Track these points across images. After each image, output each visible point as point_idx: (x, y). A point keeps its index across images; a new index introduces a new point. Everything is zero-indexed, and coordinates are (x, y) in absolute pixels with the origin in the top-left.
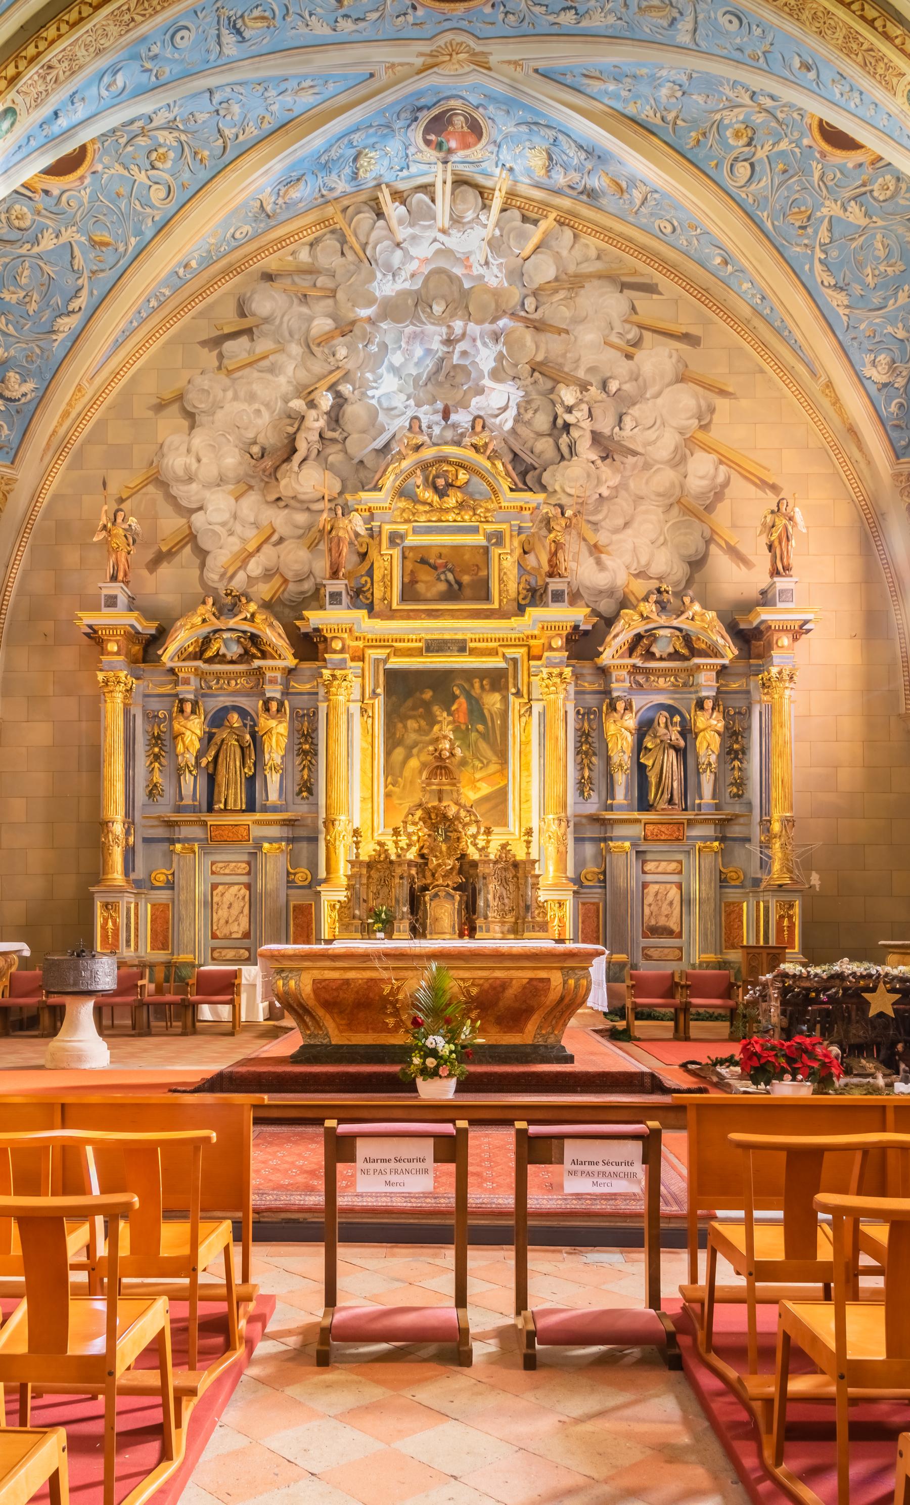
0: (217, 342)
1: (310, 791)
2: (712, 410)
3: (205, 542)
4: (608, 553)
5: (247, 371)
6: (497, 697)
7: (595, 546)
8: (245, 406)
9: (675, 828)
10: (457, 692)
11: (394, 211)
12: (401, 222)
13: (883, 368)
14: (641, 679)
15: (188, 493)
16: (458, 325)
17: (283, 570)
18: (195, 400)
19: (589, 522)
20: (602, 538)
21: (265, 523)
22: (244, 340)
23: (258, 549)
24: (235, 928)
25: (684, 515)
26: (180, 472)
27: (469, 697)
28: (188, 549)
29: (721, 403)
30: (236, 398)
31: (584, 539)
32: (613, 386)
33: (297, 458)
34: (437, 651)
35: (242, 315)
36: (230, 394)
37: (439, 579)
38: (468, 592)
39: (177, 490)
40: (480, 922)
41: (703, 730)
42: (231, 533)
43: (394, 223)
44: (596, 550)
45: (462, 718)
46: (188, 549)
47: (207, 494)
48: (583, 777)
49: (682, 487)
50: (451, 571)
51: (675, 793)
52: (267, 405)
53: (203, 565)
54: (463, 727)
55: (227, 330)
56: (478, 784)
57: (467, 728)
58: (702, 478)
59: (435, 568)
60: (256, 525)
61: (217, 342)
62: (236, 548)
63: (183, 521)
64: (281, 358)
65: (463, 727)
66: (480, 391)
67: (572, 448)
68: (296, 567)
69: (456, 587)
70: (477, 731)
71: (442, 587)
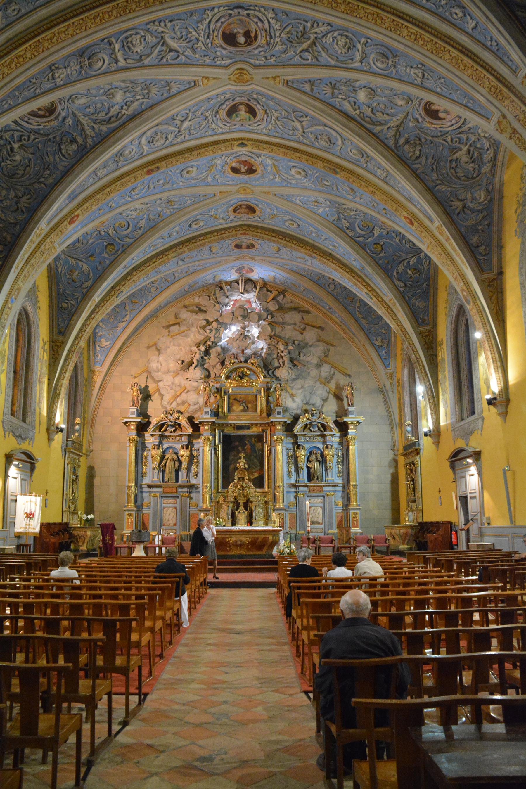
0: (168, 327)
1: (197, 475)
2: (329, 351)
3: (163, 392)
5: (178, 336)
8: (177, 348)
11: (226, 288)
12: (228, 290)
13: (380, 341)
14: (307, 438)
15: (158, 375)
16: (246, 323)
17: (189, 401)
18: (161, 345)
20: (294, 391)
21: (183, 386)
22: (177, 327)
23: (180, 394)
24: (171, 522)
26: (155, 368)
27: (251, 444)
28: (157, 394)
29: (332, 349)
30: (174, 345)
32: (296, 343)
33: (194, 365)
35: (176, 318)
36: (172, 344)
38: (250, 410)
39: (154, 374)
40: (254, 520)
42: (172, 389)
43: (226, 291)
44: (292, 395)
45: (248, 451)
46: (157, 394)
47: (164, 376)
49: (320, 375)
52: (184, 347)
53: (162, 399)
55: (171, 323)
59: (239, 401)
60: (180, 386)
61: (168, 327)
62: (173, 394)
63: (155, 385)
64: (190, 332)
66: (254, 343)
67: (283, 363)
68: (193, 400)
71: (242, 408)
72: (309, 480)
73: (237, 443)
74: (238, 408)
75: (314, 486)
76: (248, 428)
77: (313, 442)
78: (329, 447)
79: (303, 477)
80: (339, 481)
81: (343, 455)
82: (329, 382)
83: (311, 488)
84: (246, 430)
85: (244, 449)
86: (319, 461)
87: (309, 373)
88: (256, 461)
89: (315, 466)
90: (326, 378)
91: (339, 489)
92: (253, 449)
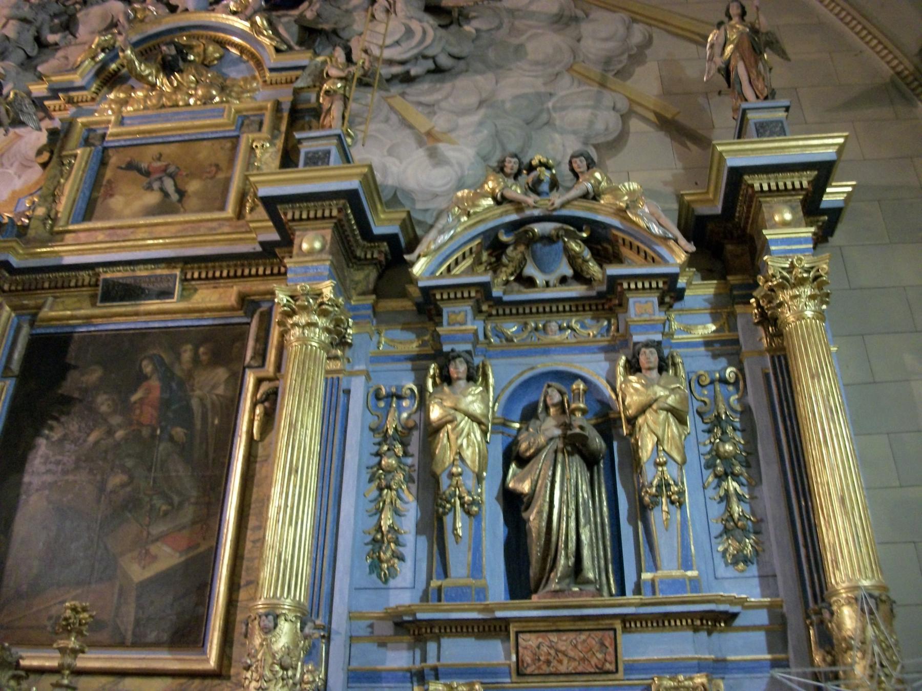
4: (451, 142)
6: (221, 373)
7: (429, 134)
9: (593, 640)
10: (148, 368)
19: (420, 104)
20: (440, 123)
25: (580, 83)
27: (167, 375)
31: (410, 127)
34: (122, 299)
37: (149, 188)
41: (642, 411)
48: (379, 529)
50: (172, 176)
51: (586, 552)
54: (145, 432)
56: (153, 549)
57: (153, 436)
58: (606, 40)
59: (147, 174)
65: (145, 432)
69: (175, 197)
70: (171, 439)
71: (153, 198)
72: (521, 584)
73: (94, 375)
74: (129, 202)
75: (552, 626)
76: (166, 294)
77: (546, 350)
78: (649, 358)
79: (476, 568)
80: (742, 588)
81: (746, 412)
82: (623, 74)
83: (530, 641)
84: (154, 305)
85: (124, 407)
86: (591, 461)
87: (519, 50)
88: (180, 471)
89: (562, 495)
90: (607, 62)
91: (747, 646)
92: (175, 406)
